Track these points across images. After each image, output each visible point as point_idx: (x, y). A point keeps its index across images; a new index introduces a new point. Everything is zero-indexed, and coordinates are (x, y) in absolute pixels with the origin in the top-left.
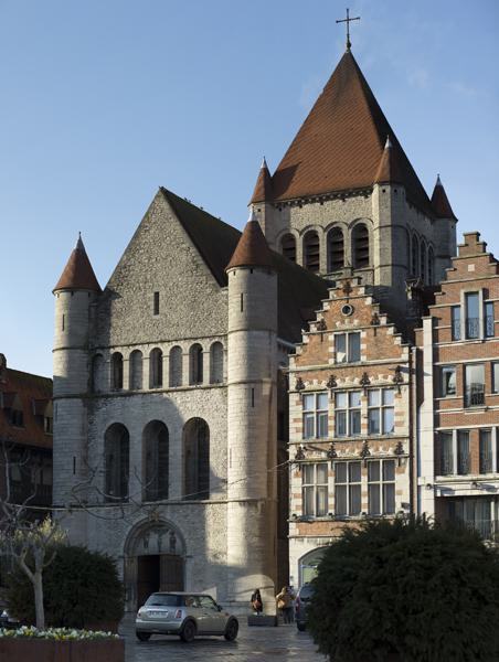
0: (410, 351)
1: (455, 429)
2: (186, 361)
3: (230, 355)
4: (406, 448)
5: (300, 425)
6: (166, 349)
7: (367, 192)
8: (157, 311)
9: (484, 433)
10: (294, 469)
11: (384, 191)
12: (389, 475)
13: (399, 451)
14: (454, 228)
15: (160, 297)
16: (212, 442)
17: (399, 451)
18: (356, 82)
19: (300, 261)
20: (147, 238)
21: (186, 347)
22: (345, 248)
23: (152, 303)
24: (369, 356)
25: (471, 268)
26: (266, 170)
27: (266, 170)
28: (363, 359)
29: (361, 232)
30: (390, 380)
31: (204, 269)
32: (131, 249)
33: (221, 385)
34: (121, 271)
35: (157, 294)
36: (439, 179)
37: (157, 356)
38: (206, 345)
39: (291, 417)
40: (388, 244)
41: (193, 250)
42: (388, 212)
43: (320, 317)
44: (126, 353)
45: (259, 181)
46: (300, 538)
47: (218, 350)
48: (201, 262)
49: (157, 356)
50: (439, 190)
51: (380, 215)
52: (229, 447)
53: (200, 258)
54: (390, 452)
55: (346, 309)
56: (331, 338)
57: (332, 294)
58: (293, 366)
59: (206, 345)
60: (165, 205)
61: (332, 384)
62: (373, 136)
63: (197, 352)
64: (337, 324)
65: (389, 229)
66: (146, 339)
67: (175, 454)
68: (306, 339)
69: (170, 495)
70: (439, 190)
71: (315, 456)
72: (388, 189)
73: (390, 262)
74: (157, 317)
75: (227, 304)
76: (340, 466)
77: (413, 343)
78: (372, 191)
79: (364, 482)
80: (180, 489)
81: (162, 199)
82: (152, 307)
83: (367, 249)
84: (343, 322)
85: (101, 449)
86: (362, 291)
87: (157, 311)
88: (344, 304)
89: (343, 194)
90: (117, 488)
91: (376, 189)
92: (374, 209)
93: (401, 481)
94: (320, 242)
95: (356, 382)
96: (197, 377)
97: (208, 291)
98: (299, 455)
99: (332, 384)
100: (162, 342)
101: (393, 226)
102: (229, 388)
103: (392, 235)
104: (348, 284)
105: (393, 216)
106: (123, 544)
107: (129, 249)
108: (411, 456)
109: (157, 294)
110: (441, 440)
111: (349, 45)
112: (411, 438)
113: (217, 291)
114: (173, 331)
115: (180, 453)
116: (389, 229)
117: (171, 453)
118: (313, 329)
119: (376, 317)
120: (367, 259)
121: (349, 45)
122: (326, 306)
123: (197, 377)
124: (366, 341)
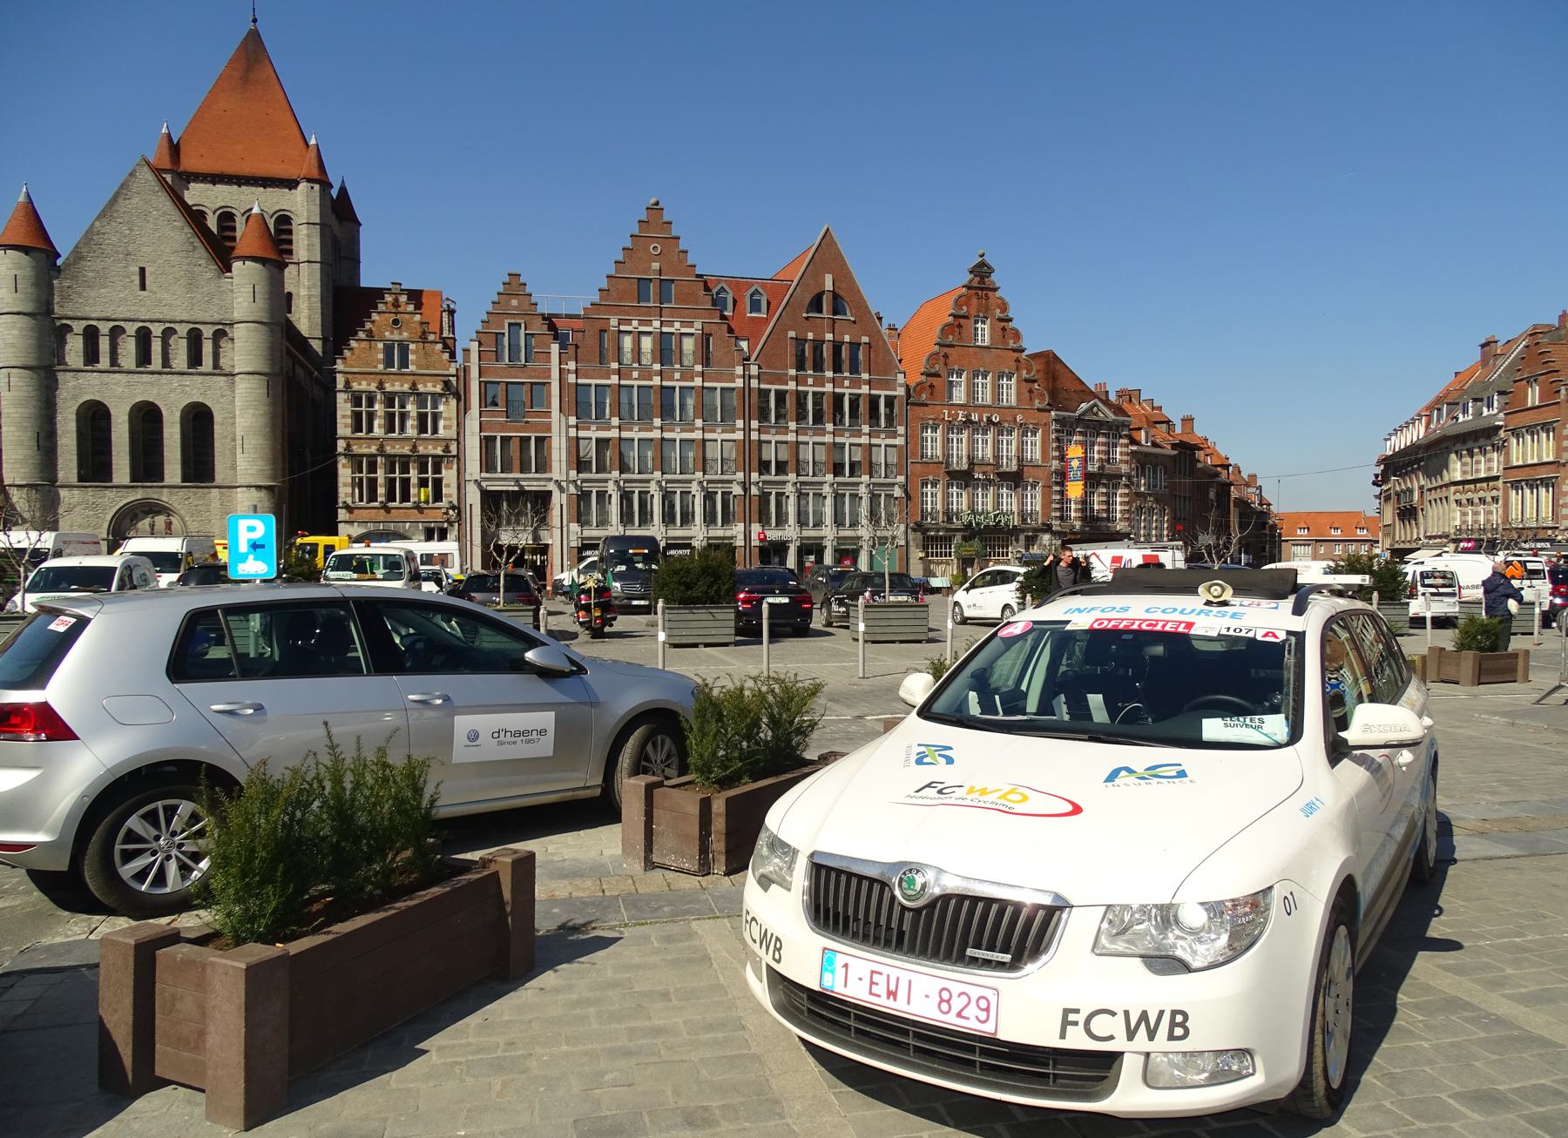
1: (499, 435)
2: (184, 343)
4: (453, 449)
5: (349, 421)
6: (157, 330)
7: (291, 184)
8: (143, 287)
9: (525, 441)
10: (342, 461)
12: (437, 470)
13: (447, 449)
16: (217, 428)
17: (447, 449)
20: (123, 205)
21: (182, 330)
24: (419, 367)
25: (514, 302)
26: (169, 135)
27: (169, 135)
28: (412, 368)
30: (438, 389)
31: (201, 255)
32: (108, 212)
33: (228, 369)
34: (89, 236)
35: (142, 270)
37: (144, 337)
38: (208, 332)
39: (339, 413)
40: (317, 241)
41: (187, 230)
43: (368, 326)
44: (104, 328)
46: (351, 522)
47: (219, 335)
48: (198, 243)
49: (144, 337)
52: (239, 433)
54: (439, 451)
55: (396, 322)
56: (380, 345)
57: (381, 307)
58: (340, 366)
59: (208, 332)
60: (147, 175)
61: (381, 386)
63: (195, 339)
66: (128, 315)
67: (172, 434)
68: (353, 344)
70: (343, 191)
71: (364, 450)
72: (317, 187)
76: (391, 461)
78: (295, 188)
79: (380, 474)
80: (179, 472)
82: (137, 282)
83: (290, 242)
85: (73, 426)
86: (411, 308)
87: (143, 287)
88: (393, 317)
90: (95, 468)
91: (303, 186)
92: (302, 204)
93: (449, 475)
94: (238, 226)
95: (406, 388)
96: (195, 359)
97: (209, 275)
98: (349, 446)
99: (381, 386)
100: (152, 321)
101: (324, 226)
102: (237, 378)
104: (396, 300)
106: (106, 525)
107: (102, 215)
108: (457, 456)
109: (142, 270)
110: (487, 443)
111: (255, 21)
112: (457, 440)
114: (165, 310)
115: (177, 437)
118: (362, 335)
119: (424, 333)
121: (255, 21)
122: (375, 316)
123: (195, 359)
124: (414, 352)
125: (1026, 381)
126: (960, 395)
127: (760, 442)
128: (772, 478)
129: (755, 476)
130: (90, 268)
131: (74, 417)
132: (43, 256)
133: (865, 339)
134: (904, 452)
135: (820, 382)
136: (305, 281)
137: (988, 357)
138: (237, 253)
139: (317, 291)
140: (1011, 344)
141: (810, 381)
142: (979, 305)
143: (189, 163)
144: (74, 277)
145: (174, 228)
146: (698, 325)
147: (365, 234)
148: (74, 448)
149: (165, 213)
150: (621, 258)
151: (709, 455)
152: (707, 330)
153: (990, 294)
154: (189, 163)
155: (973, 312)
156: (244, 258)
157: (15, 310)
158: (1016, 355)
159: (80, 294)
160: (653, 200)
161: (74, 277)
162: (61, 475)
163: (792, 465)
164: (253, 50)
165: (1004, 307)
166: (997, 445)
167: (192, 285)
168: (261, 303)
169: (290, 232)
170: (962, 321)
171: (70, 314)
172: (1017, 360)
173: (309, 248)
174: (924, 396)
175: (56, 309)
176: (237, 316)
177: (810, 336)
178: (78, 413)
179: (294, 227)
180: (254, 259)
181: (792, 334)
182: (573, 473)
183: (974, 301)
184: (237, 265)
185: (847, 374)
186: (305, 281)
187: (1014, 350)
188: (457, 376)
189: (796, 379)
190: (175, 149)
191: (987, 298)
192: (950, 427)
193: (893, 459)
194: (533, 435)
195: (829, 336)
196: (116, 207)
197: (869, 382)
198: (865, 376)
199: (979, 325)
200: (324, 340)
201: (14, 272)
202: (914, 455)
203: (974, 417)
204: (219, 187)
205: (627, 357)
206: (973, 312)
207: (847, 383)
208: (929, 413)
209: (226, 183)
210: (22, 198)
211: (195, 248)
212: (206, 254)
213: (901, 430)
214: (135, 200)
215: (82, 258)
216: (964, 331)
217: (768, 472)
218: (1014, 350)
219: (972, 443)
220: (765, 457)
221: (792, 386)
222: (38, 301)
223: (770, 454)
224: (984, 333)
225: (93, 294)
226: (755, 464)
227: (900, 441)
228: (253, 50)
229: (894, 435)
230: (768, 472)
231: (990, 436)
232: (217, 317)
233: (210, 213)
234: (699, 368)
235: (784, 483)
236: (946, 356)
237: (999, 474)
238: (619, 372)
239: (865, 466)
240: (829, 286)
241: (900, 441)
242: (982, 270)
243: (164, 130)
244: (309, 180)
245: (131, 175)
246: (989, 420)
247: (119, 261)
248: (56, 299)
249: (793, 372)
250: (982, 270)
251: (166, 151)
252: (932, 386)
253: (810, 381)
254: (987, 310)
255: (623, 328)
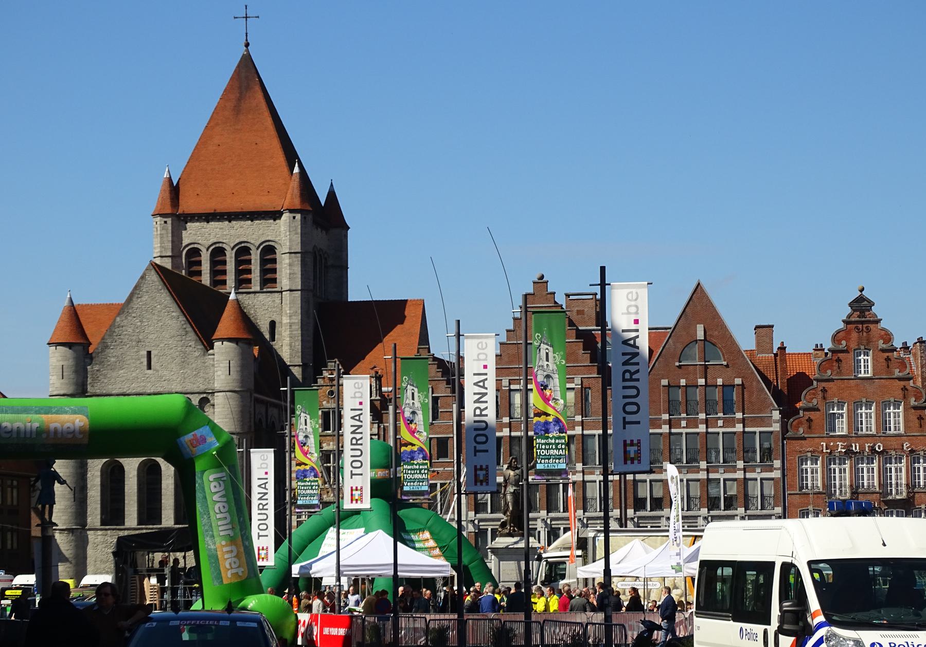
0: (379, 427)
3: (217, 409)
7: (275, 215)
8: (149, 367)
11: (294, 218)
14: (346, 236)
15: (152, 356)
18: (260, 95)
19: (206, 279)
20: (136, 303)
22: (253, 268)
23: (145, 360)
26: (170, 179)
29: (269, 251)
31: (192, 335)
35: (149, 353)
36: (332, 185)
40: (298, 269)
41: (182, 318)
42: (298, 239)
45: (163, 191)
48: (189, 329)
50: (332, 195)
51: (290, 240)
53: (189, 326)
60: (153, 277)
62: (280, 158)
64: (324, 403)
65: (299, 255)
69: (163, 520)
70: (332, 195)
73: (299, 288)
74: (149, 371)
75: (213, 365)
77: (381, 421)
78: (280, 218)
80: (172, 516)
81: (153, 272)
82: (145, 363)
83: (274, 271)
84: (328, 402)
85: (98, 481)
87: (149, 367)
88: (328, 389)
89: (253, 216)
91: (286, 216)
92: (285, 234)
97: (197, 354)
101: (304, 254)
103: (302, 261)
105: (303, 243)
109: (149, 353)
111: (247, 45)
113: (204, 355)
116: (299, 255)
117: (163, 486)
120: (274, 281)
121: (247, 45)
125: (915, 408)
126: (842, 427)
127: (635, 482)
128: (647, 513)
129: (630, 512)
130: (112, 355)
131: (99, 474)
132: (81, 348)
133: (738, 381)
134: (782, 484)
135: (693, 423)
136: (287, 309)
137: (869, 387)
138: (218, 334)
139: (297, 319)
140: (897, 373)
141: (684, 423)
142: (859, 338)
143: (188, 205)
144: (101, 363)
145: (172, 317)
146: (578, 380)
147: (353, 238)
148: (99, 498)
149: (166, 307)
150: (512, 328)
151: (589, 494)
152: (586, 384)
153: (872, 326)
154: (188, 205)
155: (853, 345)
156: (222, 340)
157: (62, 392)
158: (902, 383)
159: (105, 376)
160: (538, 275)
161: (101, 363)
162: (89, 520)
163: (666, 501)
164: (247, 76)
165: (887, 337)
166: (884, 473)
167: (184, 363)
168: (235, 375)
169: (274, 261)
170: (841, 355)
171: (98, 391)
172: (904, 389)
173: (291, 277)
174: (801, 430)
175: (89, 388)
176: (217, 385)
177: (683, 382)
178: (102, 471)
179: (278, 256)
180: (230, 340)
181: (665, 382)
182: (472, 514)
183: (854, 335)
184: (217, 344)
185: (721, 415)
186: (287, 309)
187: (900, 379)
188: (378, 434)
189: (670, 423)
190: (174, 191)
191: (868, 330)
192: (831, 458)
193: (770, 490)
194: (439, 482)
195: (702, 381)
196: (132, 305)
197: (743, 421)
198: (739, 415)
199: (862, 357)
200: (304, 366)
201: (61, 363)
202: (792, 487)
203: (856, 448)
204: (213, 224)
205: (517, 412)
206: (853, 345)
207: (720, 423)
208: (807, 446)
209: (219, 220)
210: (66, 303)
211: (187, 332)
212: (195, 337)
213: (777, 463)
214: (145, 298)
215: (107, 347)
216: (843, 364)
217: (644, 508)
218: (900, 379)
219: (856, 473)
220: (641, 495)
221: (665, 429)
222: (77, 384)
223: (644, 492)
224: (866, 365)
225: (114, 374)
226: (631, 501)
227: (777, 474)
228: (247, 76)
229: (771, 469)
230: (644, 508)
231: (875, 465)
232: (202, 388)
233: (204, 250)
234: (578, 418)
235: (659, 518)
236: (824, 391)
237: (887, 503)
238: (510, 425)
239: (741, 500)
240: (700, 335)
241: (777, 474)
242: (861, 305)
243: (166, 175)
244: (291, 211)
245: (143, 278)
246: (873, 450)
247: (133, 347)
248: (89, 381)
249: (666, 417)
250: (861, 305)
251: (167, 195)
252: (810, 420)
253: (684, 423)
254: (869, 341)
255: (512, 387)
